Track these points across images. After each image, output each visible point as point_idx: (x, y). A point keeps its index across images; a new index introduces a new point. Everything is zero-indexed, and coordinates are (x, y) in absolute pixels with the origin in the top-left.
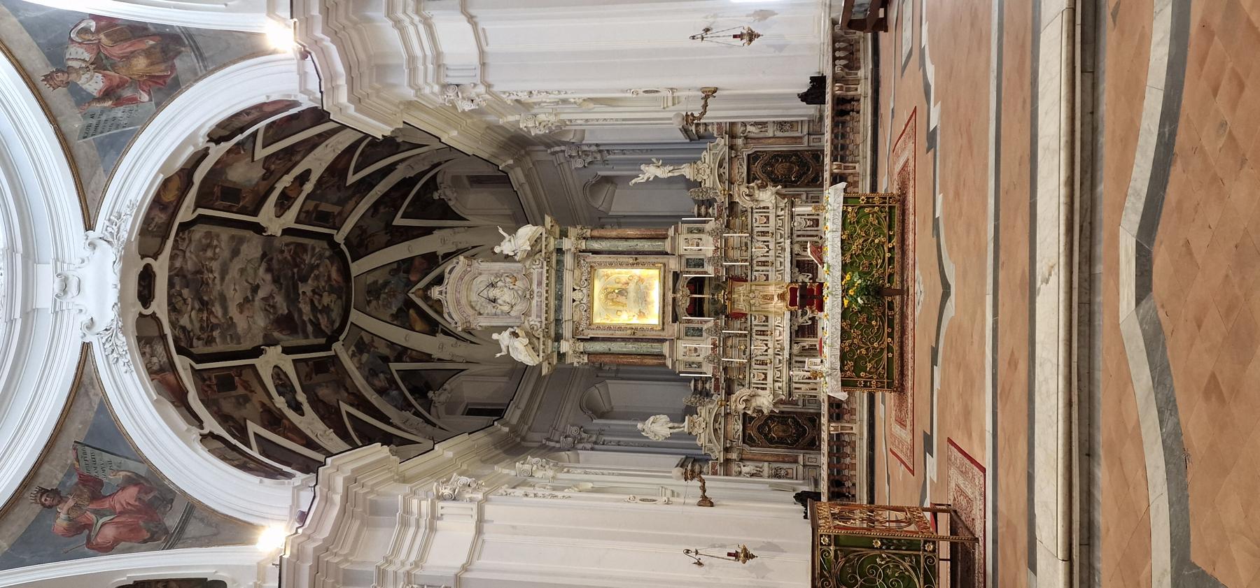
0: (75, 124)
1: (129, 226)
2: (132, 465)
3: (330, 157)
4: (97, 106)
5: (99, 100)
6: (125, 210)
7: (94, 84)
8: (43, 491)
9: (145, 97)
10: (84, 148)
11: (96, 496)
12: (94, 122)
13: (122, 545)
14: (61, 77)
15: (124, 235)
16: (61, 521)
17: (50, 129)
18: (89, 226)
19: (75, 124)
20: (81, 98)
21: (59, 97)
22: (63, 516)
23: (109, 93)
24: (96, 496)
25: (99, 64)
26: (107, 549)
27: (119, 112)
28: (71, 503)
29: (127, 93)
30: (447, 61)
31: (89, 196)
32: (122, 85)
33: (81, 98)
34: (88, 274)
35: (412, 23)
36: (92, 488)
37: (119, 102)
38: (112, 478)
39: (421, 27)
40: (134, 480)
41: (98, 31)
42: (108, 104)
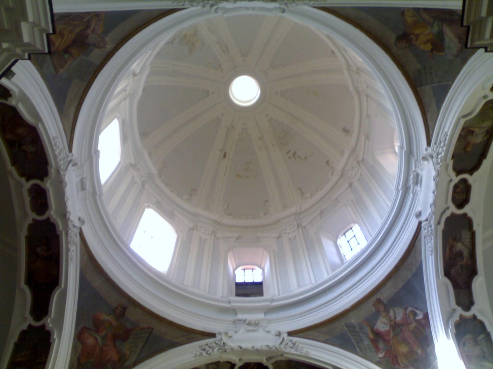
0: (353, 319)
2: (133, 359)
4: (368, 330)
5: (373, 331)
7: (382, 326)
8: (125, 309)
9: (381, 355)
10: (340, 326)
11: (115, 338)
12: (358, 329)
13: (80, 347)
14: (382, 308)
16: (104, 317)
17: (348, 306)
18: (290, 334)
19: (353, 319)
20: (371, 321)
21: (369, 308)
22: (107, 318)
23: (378, 336)
24: (115, 338)
25: (395, 326)
26: (79, 336)
27: (367, 342)
28: (115, 323)
29: (381, 345)
31: (310, 333)
32: (386, 341)
33: (371, 321)
34: (260, 334)
36: (123, 335)
37: (374, 342)
38: (126, 348)
40: (122, 359)
41: (418, 321)
42: (371, 336)
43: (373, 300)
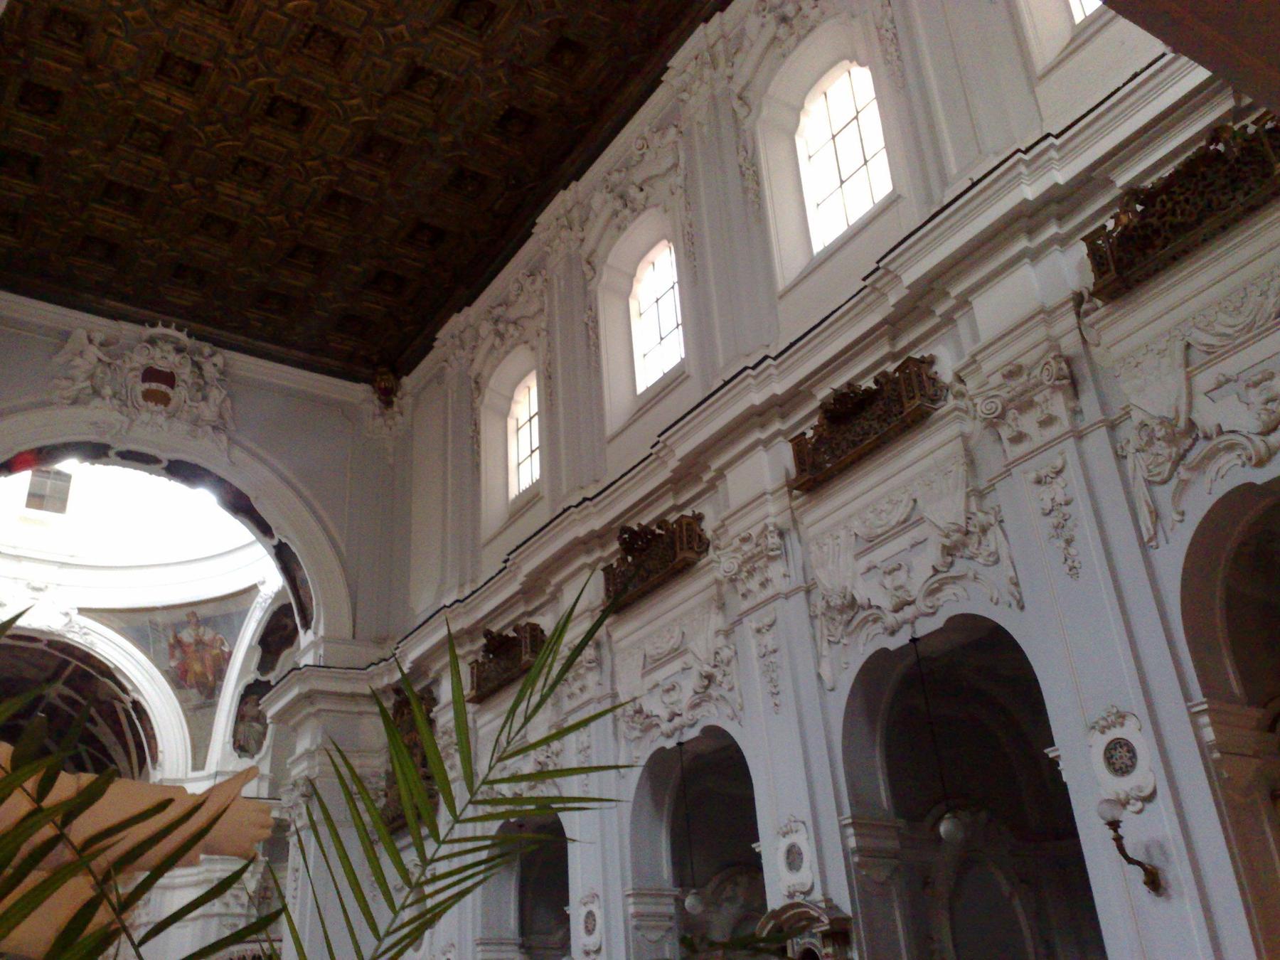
1: (75, 638)
3: (103, 739)
5: (175, 637)
6: (89, 638)
7: (187, 636)
9: (173, 664)
12: (160, 629)
14: (194, 620)
15: (70, 636)
18: (82, 611)
20: (177, 627)
21: (182, 615)
23: (179, 643)
25: (199, 642)
27: (164, 645)
29: (178, 653)
30: (168, 894)
31: (105, 615)
32: (184, 652)
35: (199, 874)
37: (172, 647)
39: (196, 878)
41: (222, 651)
42: (172, 641)
43: (190, 609)
